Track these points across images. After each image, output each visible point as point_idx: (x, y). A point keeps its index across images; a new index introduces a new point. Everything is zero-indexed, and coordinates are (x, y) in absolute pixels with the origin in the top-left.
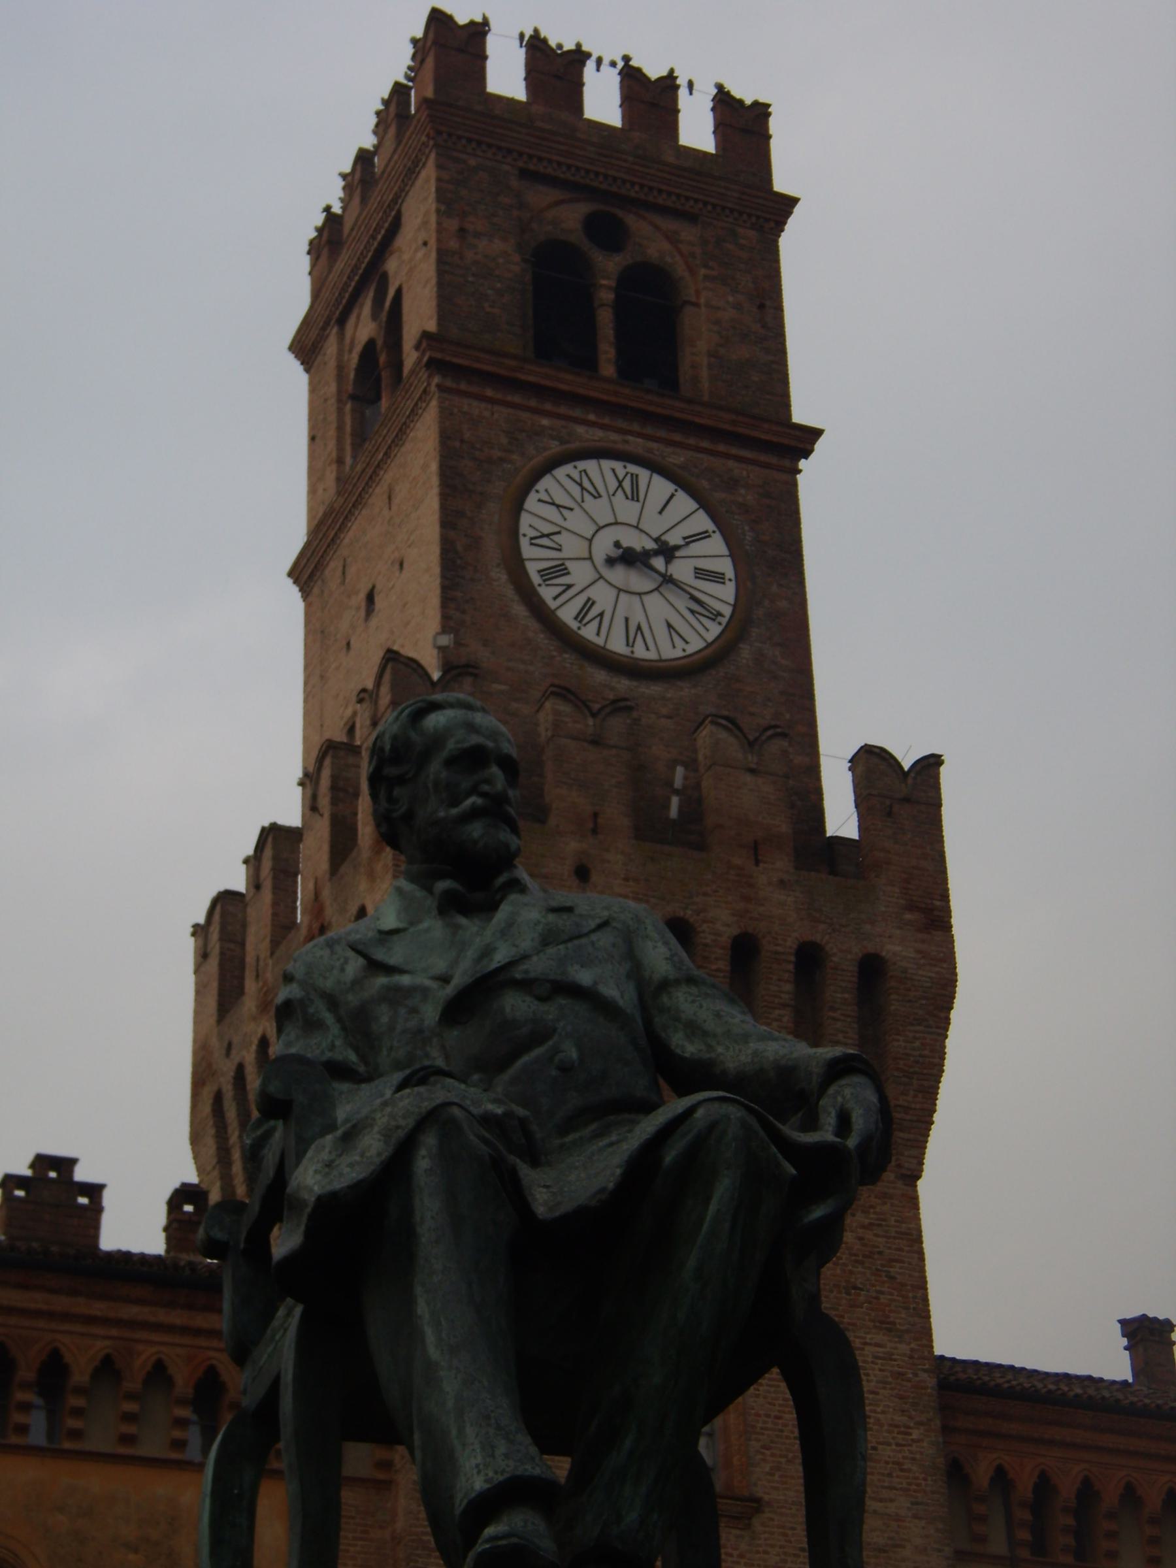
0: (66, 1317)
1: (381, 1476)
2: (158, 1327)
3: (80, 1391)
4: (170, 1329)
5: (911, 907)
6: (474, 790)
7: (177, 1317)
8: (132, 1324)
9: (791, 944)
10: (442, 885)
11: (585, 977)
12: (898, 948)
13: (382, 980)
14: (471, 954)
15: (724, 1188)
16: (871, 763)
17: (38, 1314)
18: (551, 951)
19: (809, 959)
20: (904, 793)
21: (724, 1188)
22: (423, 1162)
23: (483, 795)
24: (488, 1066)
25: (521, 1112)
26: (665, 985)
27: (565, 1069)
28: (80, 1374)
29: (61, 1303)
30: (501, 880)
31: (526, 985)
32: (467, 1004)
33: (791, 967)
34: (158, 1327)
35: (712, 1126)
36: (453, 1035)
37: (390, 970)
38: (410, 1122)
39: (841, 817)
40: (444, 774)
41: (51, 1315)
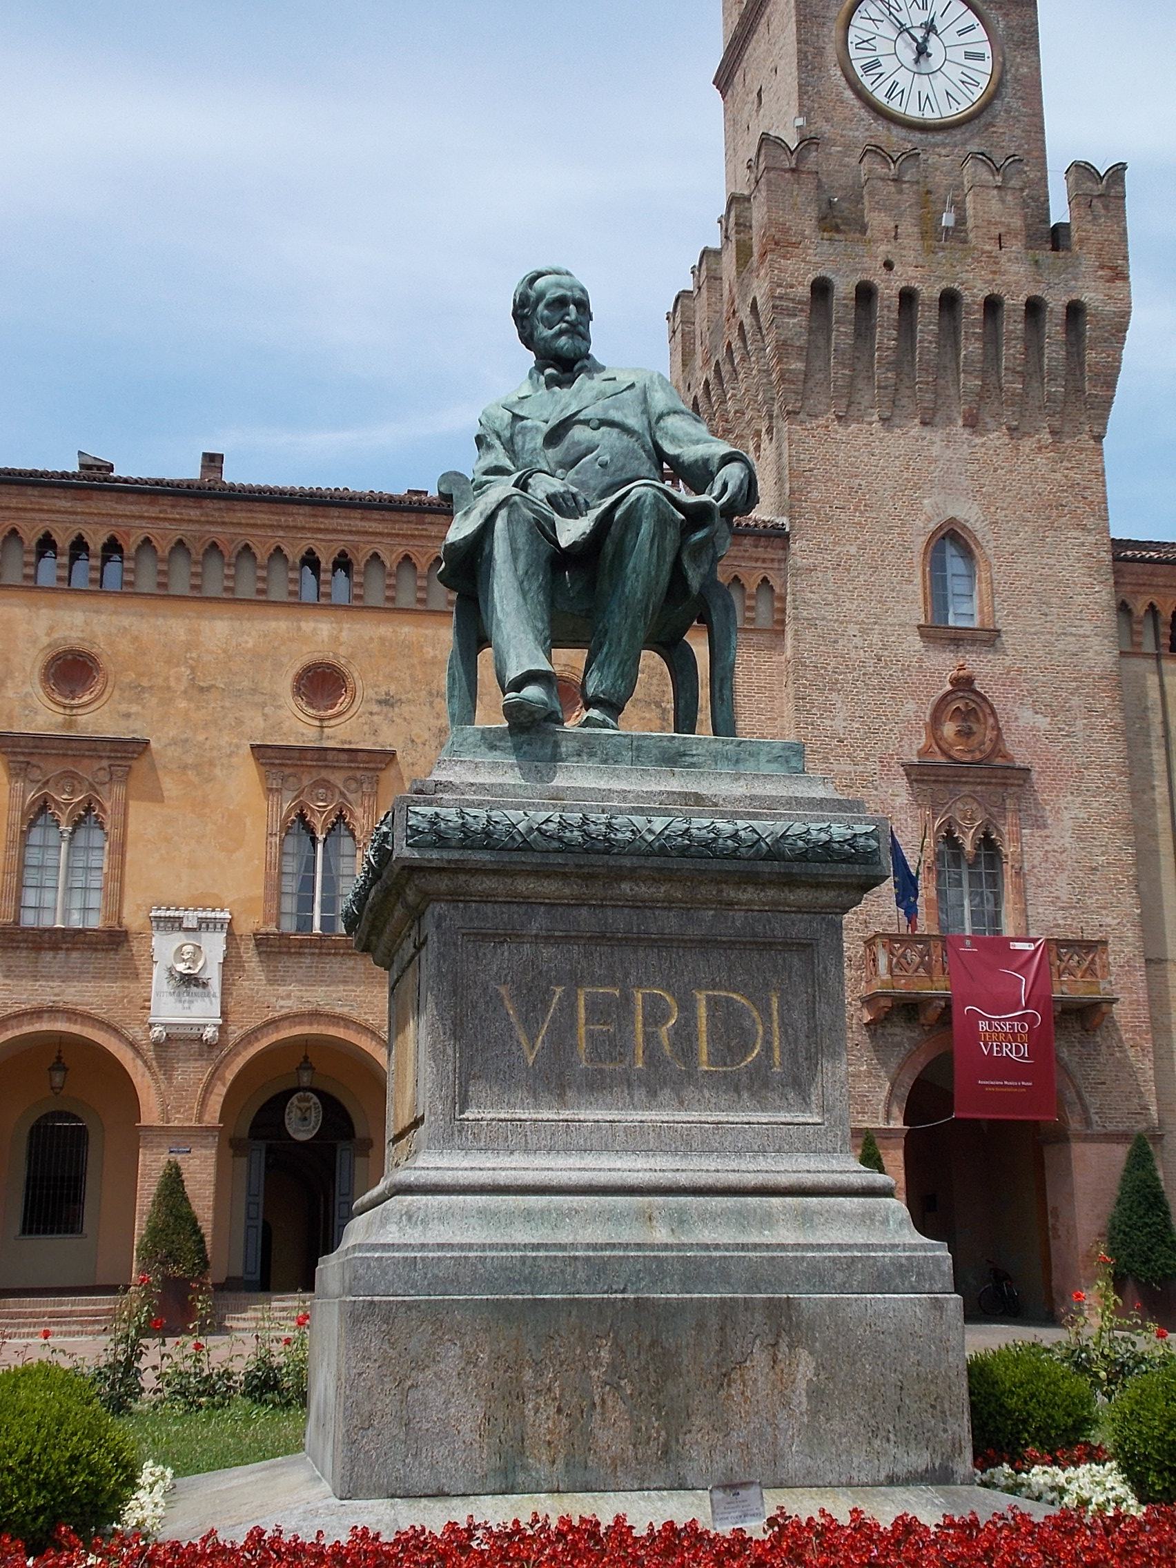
5: (1102, 267)
6: (562, 320)
9: (1023, 298)
10: (549, 371)
11: (615, 415)
12: (1092, 295)
14: (558, 408)
15: (646, 528)
16: (1081, 170)
18: (600, 402)
19: (1034, 308)
20: (1102, 188)
21: (646, 528)
22: (500, 524)
23: (567, 322)
24: (569, 464)
25: (574, 490)
26: (661, 417)
27: (604, 465)
30: (577, 367)
31: (586, 422)
32: (555, 436)
33: (1022, 313)
35: (639, 499)
37: (523, 418)
38: (494, 506)
39: (1059, 212)
40: (546, 312)
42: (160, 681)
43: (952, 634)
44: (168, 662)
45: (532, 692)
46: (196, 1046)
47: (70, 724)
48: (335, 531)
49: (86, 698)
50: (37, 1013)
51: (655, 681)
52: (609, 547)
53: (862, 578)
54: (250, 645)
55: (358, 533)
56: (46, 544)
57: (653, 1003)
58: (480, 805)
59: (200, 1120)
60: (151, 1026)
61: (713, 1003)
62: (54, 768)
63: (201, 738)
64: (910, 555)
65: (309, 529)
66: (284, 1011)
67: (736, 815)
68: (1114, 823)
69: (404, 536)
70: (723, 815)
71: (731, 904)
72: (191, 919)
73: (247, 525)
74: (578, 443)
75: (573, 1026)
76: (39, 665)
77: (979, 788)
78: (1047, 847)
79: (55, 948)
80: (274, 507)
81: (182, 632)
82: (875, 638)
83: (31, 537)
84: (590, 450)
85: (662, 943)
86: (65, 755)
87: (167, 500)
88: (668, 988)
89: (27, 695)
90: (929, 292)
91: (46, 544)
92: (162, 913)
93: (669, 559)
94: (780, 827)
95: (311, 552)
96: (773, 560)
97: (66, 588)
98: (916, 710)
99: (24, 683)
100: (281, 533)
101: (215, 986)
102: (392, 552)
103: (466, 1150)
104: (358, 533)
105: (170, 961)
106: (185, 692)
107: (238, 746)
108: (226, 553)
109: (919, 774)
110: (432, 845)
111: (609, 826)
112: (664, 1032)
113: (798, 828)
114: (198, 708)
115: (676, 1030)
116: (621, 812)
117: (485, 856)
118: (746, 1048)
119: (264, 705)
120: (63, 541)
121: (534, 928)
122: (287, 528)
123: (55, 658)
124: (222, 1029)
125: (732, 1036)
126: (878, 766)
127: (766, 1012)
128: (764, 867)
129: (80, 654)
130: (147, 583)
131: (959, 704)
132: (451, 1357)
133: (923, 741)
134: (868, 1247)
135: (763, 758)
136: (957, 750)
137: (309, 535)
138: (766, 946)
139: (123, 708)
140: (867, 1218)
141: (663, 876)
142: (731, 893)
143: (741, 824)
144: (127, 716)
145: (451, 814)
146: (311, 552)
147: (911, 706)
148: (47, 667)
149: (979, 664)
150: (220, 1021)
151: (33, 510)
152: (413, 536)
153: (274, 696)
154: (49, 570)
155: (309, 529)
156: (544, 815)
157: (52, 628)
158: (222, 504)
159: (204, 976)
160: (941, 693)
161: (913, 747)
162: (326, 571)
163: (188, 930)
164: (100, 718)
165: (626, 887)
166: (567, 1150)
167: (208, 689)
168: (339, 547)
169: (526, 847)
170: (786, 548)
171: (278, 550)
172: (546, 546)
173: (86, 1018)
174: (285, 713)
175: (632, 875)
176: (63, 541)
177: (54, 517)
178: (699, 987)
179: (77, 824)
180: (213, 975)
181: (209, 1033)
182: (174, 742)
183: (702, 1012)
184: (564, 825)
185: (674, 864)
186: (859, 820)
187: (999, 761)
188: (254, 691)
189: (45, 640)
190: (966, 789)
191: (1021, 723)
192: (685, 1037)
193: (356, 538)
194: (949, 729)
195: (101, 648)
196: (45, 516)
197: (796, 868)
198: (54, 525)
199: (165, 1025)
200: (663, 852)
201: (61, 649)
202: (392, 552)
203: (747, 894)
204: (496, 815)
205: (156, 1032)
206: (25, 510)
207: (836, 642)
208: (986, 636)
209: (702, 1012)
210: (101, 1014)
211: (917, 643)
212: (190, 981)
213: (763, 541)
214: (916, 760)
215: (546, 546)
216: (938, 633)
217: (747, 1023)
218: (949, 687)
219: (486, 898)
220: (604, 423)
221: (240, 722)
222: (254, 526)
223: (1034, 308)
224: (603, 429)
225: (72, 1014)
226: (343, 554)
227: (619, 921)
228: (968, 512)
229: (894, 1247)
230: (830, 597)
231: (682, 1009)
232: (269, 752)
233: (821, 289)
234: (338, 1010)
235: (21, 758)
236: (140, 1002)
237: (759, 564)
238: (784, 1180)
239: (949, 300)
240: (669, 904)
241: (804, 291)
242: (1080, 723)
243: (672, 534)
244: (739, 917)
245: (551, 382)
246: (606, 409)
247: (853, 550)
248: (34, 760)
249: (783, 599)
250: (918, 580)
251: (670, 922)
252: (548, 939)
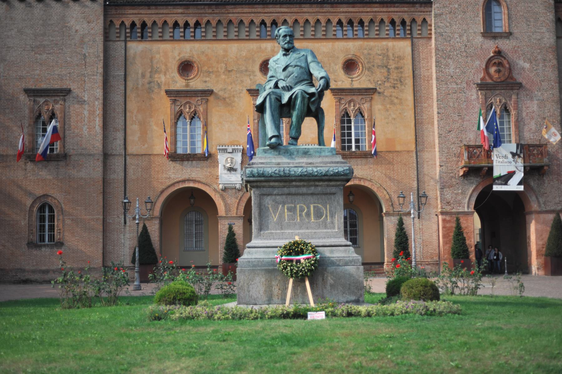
0: (362, 12)
1: (429, 36)
2: (381, 12)
3: (366, 26)
4: (384, 12)
7: (385, 9)
8: (376, 12)
11: (299, 64)
13: (277, 65)
17: (357, 12)
28: (366, 24)
29: (361, 9)
31: (291, 66)
34: (381, 12)
36: (284, 73)
41: (360, 12)
42: (215, 69)
43: (493, 35)
44: (218, 62)
45: (273, 140)
46: (234, 191)
47: (187, 85)
48: (271, 13)
49: (192, 77)
50: (184, 181)
51: (385, 58)
52: (292, 103)
53: (460, 16)
54: (244, 55)
55: (279, 13)
56: (176, 25)
57: (301, 207)
58: (261, 167)
59: (237, 214)
61: (314, 207)
62: (184, 101)
63: (230, 88)
64: (478, 6)
65: (262, 13)
67: (317, 167)
68: (553, 101)
69: (295, 12)
70: (314, 167)
71: (317, 186)
72: (230, 149)
73: (241, 13)
74: (289, 72)
75: (284, 212)
76: (176, 66)
77: (503, 91)
78: (528, 111)
79: (188, 160)
80: (250, 6)
81: (221, 51)
82: (465, 38)
83: (171, 23)
84: (292, 73)
85: (303, 194)
86: (187, 96)
87: (214, 7)
88: (304, 204)
89: (174, 76)
91: (176, 25)
92: (221, 147)
93: (306, 105)
94: (327, 169)
95: (263, 21)
96: (427, 12)
97: (184, 39)
98: (480, 64)
99: (172, 73)
100: (253, 15)
102: (291, 18)
103: (261, 239)
104: (279, 13)
105: (224, 163)
106: (224, 73)
107: (242, 90)
108: (235, 23)
109: (482, 86)
110: (251, 177)
111: (289, 171)
112: (304, 213)
113: (331, 169)
114: (228, 78)
115: (306, 213)
116: (292, 167)
117: (263, 179)
118: (321, 216)
119: (250, 75)
120: (181, 23)
121: (275, 193)
122: (254, 13)
123: (181, 64)
125: (318, 215)
126: (465, 85)
127: (326, 208)
128: (324, 178)
129: (189, 61)
130: (210, 36)
131: (496, 61)
132: (257, 279)
133: (482, 75)
134: (344, 257)
135: (326, 151)
136: (496, 76)
137: (262, 15)
138: (326, 194)
139: (204, 79)
140: (345, 251)
141: (301, 181)
142: (317, 183)
143: (318, 169)
144: (205, 82)
145: (255, 171)
146: (263, 21)
147: (477, 63)
148: (179, 67)
150: (241, 182)
151: (171, 14)
152: (298, 12)
153: (253, 72)
154: (179, 32)
155: (262, 13)
156: (275, 169)
157: (180, 54)
158: (233, 6)
159: (235, 167)
160: (489, 57)
161: (478, 77)
162: (269, 27)
163: (229, 153)
164: (197, 84)
165: (294, 183)
166: (282, 239)
167: (231, 71)
168: (272, 18)
169: (271, 176)
170: (431, 7)
171: (252, 21)
172: (278, 103)
173: (199, 182)
174: (256, 78)
175: (295, 181)
176: (181, 23)
177: (178, 15)
178: (311, 204)
179: (192, 118)
180: (238, 166)
181: (238, 186)
182: (221, 90)
183: (312, 209)
184: (279, 171)
185: (303, 178)
186: (345, 166)
187: (512, 81)
188: (246, 71)
189: (178, 58)
190: (498, 92)
191: (519, 66)
192: (308, 215)
193: (279, 14)
194: (492, 70)
195: (195, 59)
196: (175, 15)
197: (331, 178)
198: (178, 18)
200: (301, 176)
201: (183, 60)
202: (291, 18)
203: (321, 183)
204: (265, 169)
206: (168, 14)
207: (450, 41)
208: (506, 35)
209: (312, 209)
210: (204, 180)
211: (480, 39)
212: (231, 169)
213: (423, 5)
214: (479, 82)
215: (278, 103)
217: (322, 211)
218: (492, 55)
219: (264, 187)
220: (296, 66)
221: (242, 81)
222: (244, 13)
224: (296, 68)
225: (194, 181)
226: (274, 20)
227: (293, 190)
229: (349, 257)
230: (448, 24)
231: (307, 208)
232: (253, 92)
235: (173, 98)
236: (215, 177)
237: (422, 13)
238: (328, 244)
240: (304, 186)
242: (541, 65)
243: (306, 100)
244: (319, 189)
245: (284, 55)
246: (296, 62)
247: (456, 6)
248: (177, 99)
249: (431, 25)
250: (481, 15)
251: (304, 190)
252: (278, 195)
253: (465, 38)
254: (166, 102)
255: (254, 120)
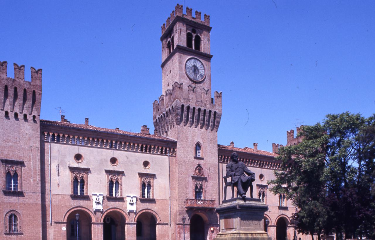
9: (209, 110)
60: (93, 209)
66: (111, 207)
90: (197, 108)
101: (102, 203)
105: (95, 200)
109: (193, 177)
124: (103, 210)
149: (201, 162)
180: (101, 202)
194: (197, 171)
199: (95, 209)
205: (94, 210)
210: (87, 207)
212: (98, 203)
216: (196, 158)
223: (210, 111)
228: (201, 141)
233: (183, 106)
234: (118, 207)
239: (199, 109)
241: (181, 106)
253: (188, 158)
254: (68, 172)
255: (108, 183)
